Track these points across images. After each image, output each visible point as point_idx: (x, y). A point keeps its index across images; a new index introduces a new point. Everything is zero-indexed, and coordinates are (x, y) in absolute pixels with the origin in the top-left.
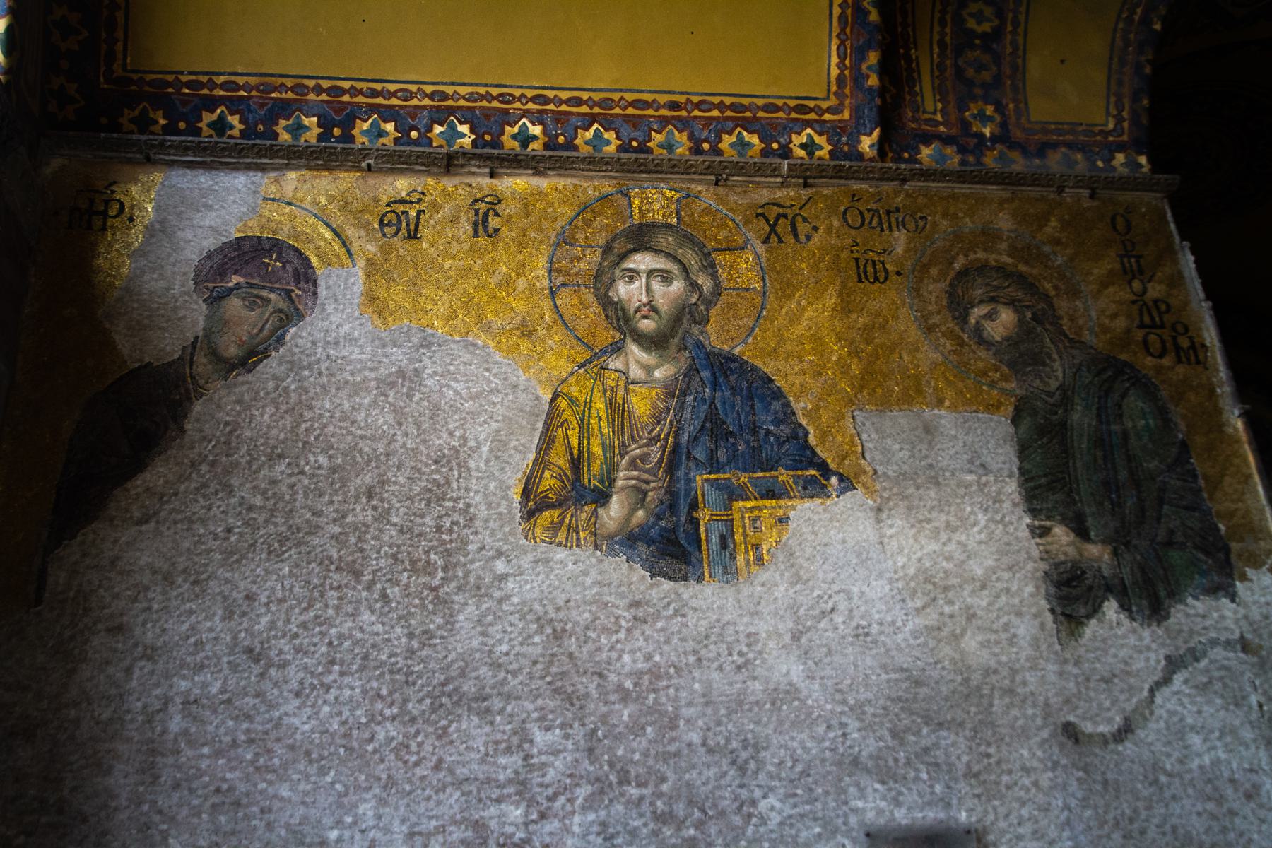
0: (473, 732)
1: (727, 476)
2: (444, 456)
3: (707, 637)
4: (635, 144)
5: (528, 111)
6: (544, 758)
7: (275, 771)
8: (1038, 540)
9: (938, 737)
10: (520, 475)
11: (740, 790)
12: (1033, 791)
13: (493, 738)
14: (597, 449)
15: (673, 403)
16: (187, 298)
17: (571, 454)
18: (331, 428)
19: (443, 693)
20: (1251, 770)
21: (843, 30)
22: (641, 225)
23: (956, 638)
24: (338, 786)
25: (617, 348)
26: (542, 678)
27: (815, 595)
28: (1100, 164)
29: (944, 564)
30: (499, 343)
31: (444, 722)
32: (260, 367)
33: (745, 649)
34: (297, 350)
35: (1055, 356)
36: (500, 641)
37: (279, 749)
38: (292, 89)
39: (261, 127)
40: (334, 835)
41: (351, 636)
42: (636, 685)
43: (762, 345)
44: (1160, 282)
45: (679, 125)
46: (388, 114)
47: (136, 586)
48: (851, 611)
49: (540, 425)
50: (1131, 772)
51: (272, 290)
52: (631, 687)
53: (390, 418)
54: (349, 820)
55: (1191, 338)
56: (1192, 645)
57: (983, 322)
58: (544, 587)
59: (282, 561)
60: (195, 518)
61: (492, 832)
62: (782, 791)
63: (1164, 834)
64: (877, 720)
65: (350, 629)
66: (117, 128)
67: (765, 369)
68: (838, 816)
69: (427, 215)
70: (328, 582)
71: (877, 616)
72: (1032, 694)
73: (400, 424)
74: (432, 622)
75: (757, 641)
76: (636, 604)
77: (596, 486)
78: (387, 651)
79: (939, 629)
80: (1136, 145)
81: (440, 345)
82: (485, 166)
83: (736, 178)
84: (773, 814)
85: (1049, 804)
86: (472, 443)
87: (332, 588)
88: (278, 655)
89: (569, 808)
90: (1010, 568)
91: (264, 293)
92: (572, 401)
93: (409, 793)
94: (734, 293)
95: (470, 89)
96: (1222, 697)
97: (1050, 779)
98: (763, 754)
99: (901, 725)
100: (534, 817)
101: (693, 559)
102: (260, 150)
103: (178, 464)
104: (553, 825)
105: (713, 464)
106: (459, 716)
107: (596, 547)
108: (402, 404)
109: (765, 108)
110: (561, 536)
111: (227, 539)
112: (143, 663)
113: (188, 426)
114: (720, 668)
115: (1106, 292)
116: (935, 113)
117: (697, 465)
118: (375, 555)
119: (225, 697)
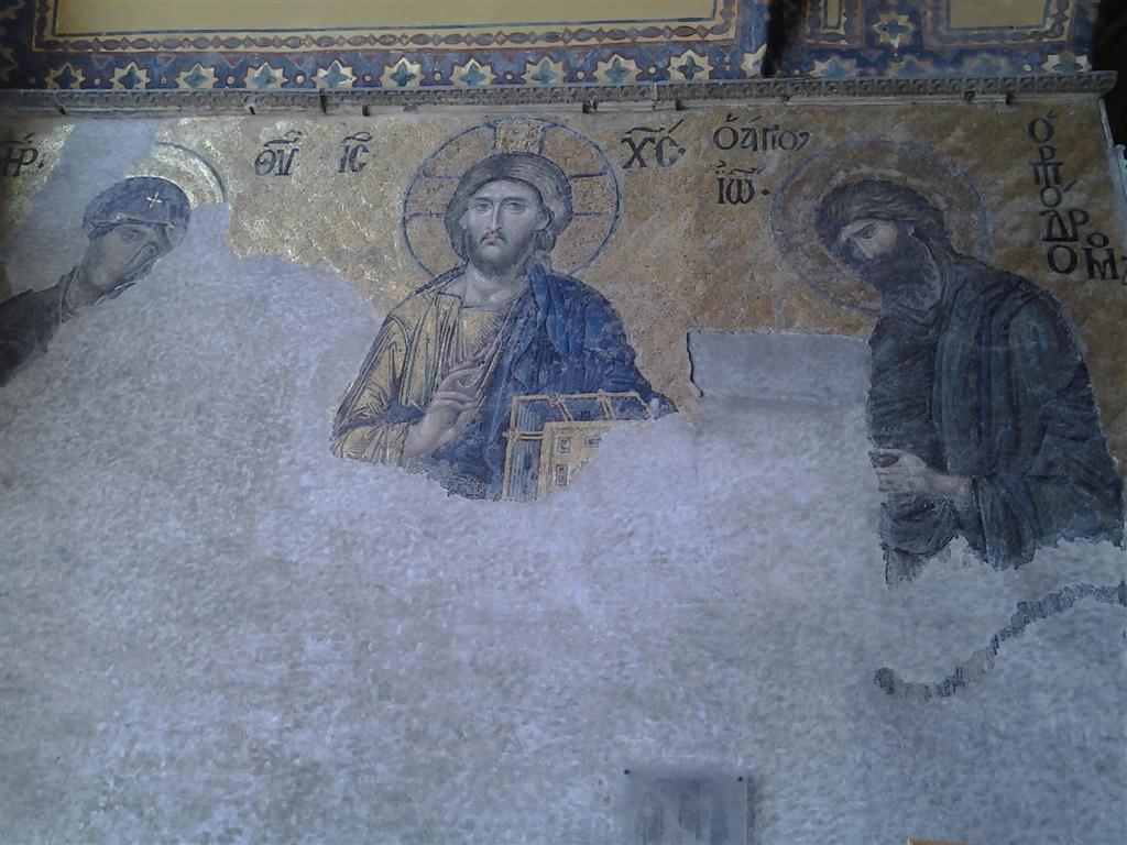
1: (545, 397)
3: (494, 556)
5: (407, 51)
6: (310, 667)
8: (881, 470)
10: (340, 393)
11: (500, 714)
12: (828, 741)
14: (420, 371)
15: (504, 327)
17: (394, 374)
18: (176, 349)
20: (1109, 739)
24: (114, 681)
25: (457, 273)
27: (615, 517)
29: (764, 492)
30: (345, 270)
31: (224, 627)
33: (532, 570)
34: (159, 278)
35: (936, 273)
38: (194, 43)
40: (101, 727)
42: (415, 600)
43: (603, 268)
44: (1081, 190)
49: (368, 348)
51: (149, 225)
54: (117, 714)
56: (1055, 591)
57: (856, 240)
58: (343, 501)
59: (108, 469)
61: (247, 737)
62: (545, 718)
64: (661, 650)
65: (156, 534)
67: (604, 292)
68: (599, 750)
70: (144, 489)
71: (678, 543)
72: (845, 635)
74: (233, 531)
76: (429, 520)
79: (747, 558)
80: (1077, 45)
83: (604, 104)
84: (530, 742)
85: (845, 758)
86: (302, 364)
87: (146, 496)
88: (87, 555)
89: (325, 718)
90: (840, 498)
91: (142, 228)
93: (176, 694)
94: (586, 217)
95: (355, 33)
96: (1084, 652)
97: (850, 730)
98: (531, 677)
100: (289, 725)
101: (494, 478)
105: (532, 385)
107: (400, 464)
108: (245, 327)
109: (645, 34)
110: (369, 452)
114: (503, 588)
116: (837, 27)
117: (516, 389)
119: (31, 592)
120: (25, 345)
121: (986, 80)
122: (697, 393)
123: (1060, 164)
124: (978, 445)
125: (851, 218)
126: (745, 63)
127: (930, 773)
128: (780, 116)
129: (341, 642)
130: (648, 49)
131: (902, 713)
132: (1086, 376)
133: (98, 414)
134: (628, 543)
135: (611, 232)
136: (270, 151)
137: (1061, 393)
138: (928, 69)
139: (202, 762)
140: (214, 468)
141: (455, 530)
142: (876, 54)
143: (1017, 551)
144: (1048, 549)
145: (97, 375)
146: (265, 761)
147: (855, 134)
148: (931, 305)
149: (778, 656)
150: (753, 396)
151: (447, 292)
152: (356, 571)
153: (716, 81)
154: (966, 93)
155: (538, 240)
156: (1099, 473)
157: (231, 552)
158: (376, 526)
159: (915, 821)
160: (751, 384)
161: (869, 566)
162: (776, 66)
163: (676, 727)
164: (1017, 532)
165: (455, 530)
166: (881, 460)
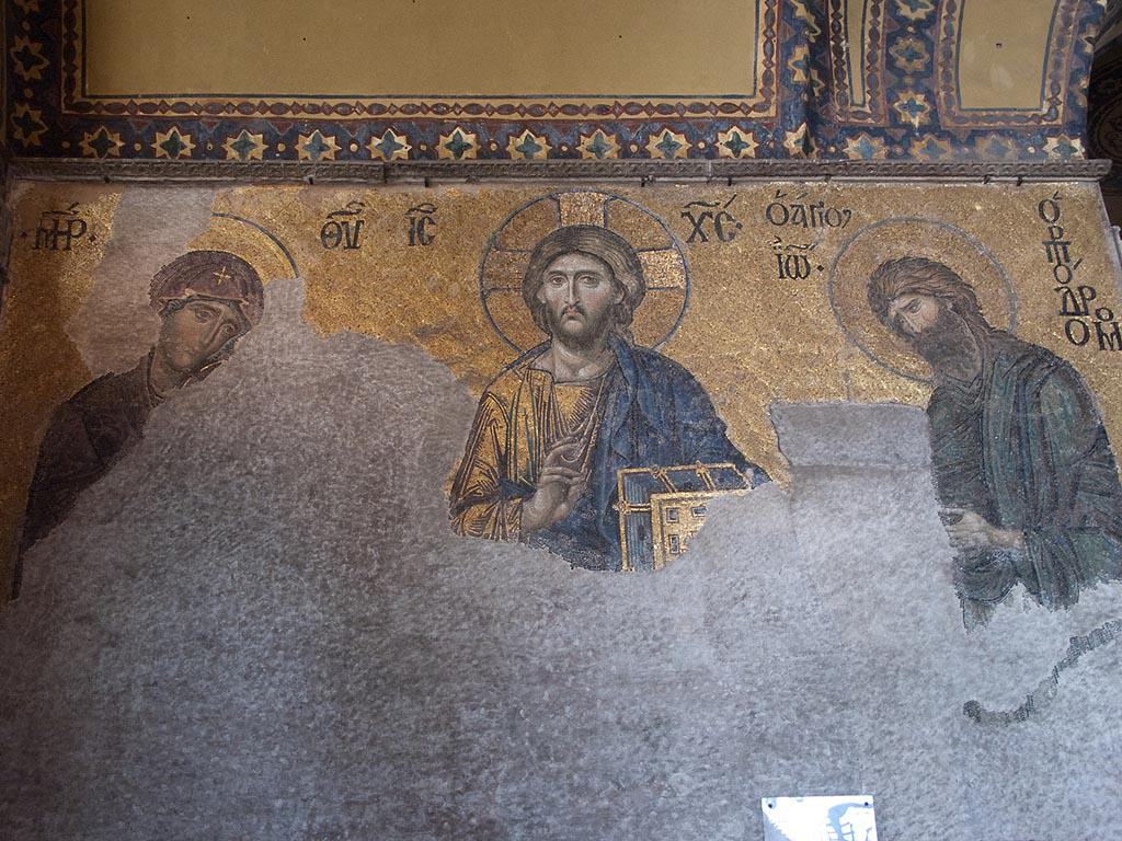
0: (404, 710)
3: (624, 623)
4: (564, 148)
5: (461, 120)
6: (469, 734)
8: (948, 527)
14: (522, 446)
17: (499, 451)
18: (276, 431)
19: (378, 676)
21: (770, 27)
25: (544, 349)
26: (469, 661)
27: (728, 582)
28: (1031, 150)
31: (379, 702)
33: (660, 634)
34: (243, 358)
35: (974, 346)
36: (431, 628)
37: (229, 726)
38: (238, 108)
39: (210, 145)
40: (279, 803)
42: (556, 667)
45: (607, 128)
46: (329, 128)
49: (470, 425)
50: (1031, 750)
51: (221, 301)
53: (330, 420)
54: (293, 790)
55: (1115, 324)
57: (903, 314)
60: (152, 517)
61: (422, 801)
62: (692, 765)
64: (785, 699)
66: (77, 152)
68: (744, 789)
70: (273, 574)
71: (787, 602)
73: (340, 426)
76: (556, 592)
78: (326, 637)
80: (1072, 128)
82: (420, 176)
86: (407, 443)
87: (276, 580)
91: (215, 305)
92: (501, 401)
93: (347, 767)
97: (950, 755)
99: (808, 706)
100: (459, 789)
102: (210, 169)
104: (475, 797)
105: (635, 460)
107: (521, 539)
109: (692, 109)
113: (145, 432)
116: (863, 105)
117: (618, 460)
123: (1068, 243)
127: (1017, 786)
129: (493, 710)
131: (989, 737)
134: (743, 606)
137: (1088, 454)
138: (947, 154)
139: (384, 829)
140: (338, 549)
141: (584, 600)
143: (1065, 596)
149: (884, 696)
152: (496, 643)
155: (615, 314)
157: (371, 631)
158: (509, 599)
159: (1009, 827)
163: (807, 765)
165: (584, 600)
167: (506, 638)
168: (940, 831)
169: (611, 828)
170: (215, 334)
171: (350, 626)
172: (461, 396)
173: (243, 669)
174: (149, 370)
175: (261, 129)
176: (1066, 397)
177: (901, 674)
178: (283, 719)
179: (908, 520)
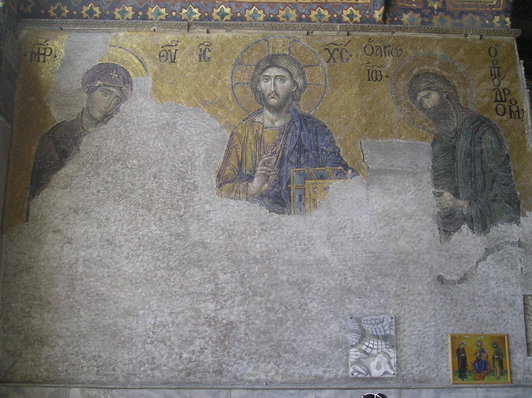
0: (196, 274)
2: (185, 160)
3: (291, 238)
4: (272, 16)
6: (223, 285)
7: (119, 288)
8: (437, 198)
9: (384, 280)
11: (301, 300)
13: (203, 277)
14: (249, 158)
15: (282, 137)
16: (79, 91)
17: (238, 160)
18: (139, 148)
19: (184, 259)
22: (272, 55)
23: (396, 239)
24: (143, 294)
25: (260, 112)
26: (223, 253)
27: (338, 221)
28: (487, 22)
29: (395, 208)
30: (209, 110)
31: (184, 270)
32: (109, 122)
33: (307, 243)
34: (124, 114)
35: (455, 115)
37: (120, 279)
39: (108, 12)
40: (141, 312)
41: (147, 235)
42: (261, 257)
45: (292, 7)
47: (63, 214)
48: (352, 228)
49: (225, 147)
51: (114, 87)
52: (259, 258)
53: (163, 143)
54: (147, 307)
56: (497, 244)
58: (225, 216)
59: (120, 204)
61: (202, 313)
62: (318, 300)
63: (473, 320)
64: (360, 273)
65: (147, 232)
68: (340, 311)
69: (179, 52)
70: (138, 213)
71: (363, 230)
72: (426, 263)
73: (167, 146)
75: (313, 240)
76: (262, 224)
77: (248, 174)
80: (506, 12)
81: (184, 111)
83: (316, 32)
86: (197, 155)
88: (119, 242)
89: (232, 305)
90: (423, 210)
92: (239, 136)
93: (170, 298)
96: (507, 265)
97: (429, 298)
100: (219, 308)
101: (287, 205)
103: (77, 164)
104: (226, 311)
105: (298, 164)
106: (190, 268)
110: (233, 195)
111: (98, 195)
112: (67, 245)
113: (81, 148)
115: (481, 85)
118: (157, 202)
119: (99, 259)
120: (69, 147)
121: (473, 30)
122: (366, 167)
123: (500, 68)
124: (471, 187)
125: (422, 89)
126: (375, 15)
127: (456, 311)
128: (391, 41)
130: (333, 5)
131: (446, 291)
132: (509, 159)
133: (110, 179)
135: (324, 93)
136: (165, 50)
137: (500, 167)
138: (449, 22)
139: (186, 324)
140: (167, 203)
141: (274, 227)
142: (428, 11)
143: (485, 229)
144: (495, 228)
145: (105, 161)
146: (211, 322)
147: (421, 50)
148: (453, 129)
150: (388, 168)
151: (256, 121)
153: (364, 25)
154: (465, 35)
156: (513, 199)
157: (181, 239)
159: (451, 328)
160: (387, 164)
161: (434, 237)
162: (388, 16)
164: (485, 222)
165: (274, 227)
166: (437, 194)
167: (240, 243)
168: (422, 329)
169: (283, 326)
170: (111, 103)
171: (171, 237)
172: (222, 134)
173: (126, 255)
174: (82, 119)
175: (131, 4)
176: (493, 140)
177: (411, 263)
178: (143, 277)
179: (419, 195)
